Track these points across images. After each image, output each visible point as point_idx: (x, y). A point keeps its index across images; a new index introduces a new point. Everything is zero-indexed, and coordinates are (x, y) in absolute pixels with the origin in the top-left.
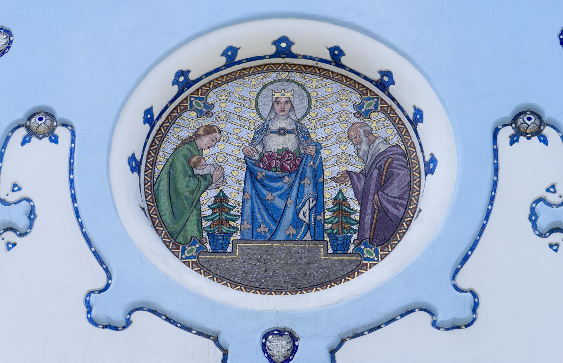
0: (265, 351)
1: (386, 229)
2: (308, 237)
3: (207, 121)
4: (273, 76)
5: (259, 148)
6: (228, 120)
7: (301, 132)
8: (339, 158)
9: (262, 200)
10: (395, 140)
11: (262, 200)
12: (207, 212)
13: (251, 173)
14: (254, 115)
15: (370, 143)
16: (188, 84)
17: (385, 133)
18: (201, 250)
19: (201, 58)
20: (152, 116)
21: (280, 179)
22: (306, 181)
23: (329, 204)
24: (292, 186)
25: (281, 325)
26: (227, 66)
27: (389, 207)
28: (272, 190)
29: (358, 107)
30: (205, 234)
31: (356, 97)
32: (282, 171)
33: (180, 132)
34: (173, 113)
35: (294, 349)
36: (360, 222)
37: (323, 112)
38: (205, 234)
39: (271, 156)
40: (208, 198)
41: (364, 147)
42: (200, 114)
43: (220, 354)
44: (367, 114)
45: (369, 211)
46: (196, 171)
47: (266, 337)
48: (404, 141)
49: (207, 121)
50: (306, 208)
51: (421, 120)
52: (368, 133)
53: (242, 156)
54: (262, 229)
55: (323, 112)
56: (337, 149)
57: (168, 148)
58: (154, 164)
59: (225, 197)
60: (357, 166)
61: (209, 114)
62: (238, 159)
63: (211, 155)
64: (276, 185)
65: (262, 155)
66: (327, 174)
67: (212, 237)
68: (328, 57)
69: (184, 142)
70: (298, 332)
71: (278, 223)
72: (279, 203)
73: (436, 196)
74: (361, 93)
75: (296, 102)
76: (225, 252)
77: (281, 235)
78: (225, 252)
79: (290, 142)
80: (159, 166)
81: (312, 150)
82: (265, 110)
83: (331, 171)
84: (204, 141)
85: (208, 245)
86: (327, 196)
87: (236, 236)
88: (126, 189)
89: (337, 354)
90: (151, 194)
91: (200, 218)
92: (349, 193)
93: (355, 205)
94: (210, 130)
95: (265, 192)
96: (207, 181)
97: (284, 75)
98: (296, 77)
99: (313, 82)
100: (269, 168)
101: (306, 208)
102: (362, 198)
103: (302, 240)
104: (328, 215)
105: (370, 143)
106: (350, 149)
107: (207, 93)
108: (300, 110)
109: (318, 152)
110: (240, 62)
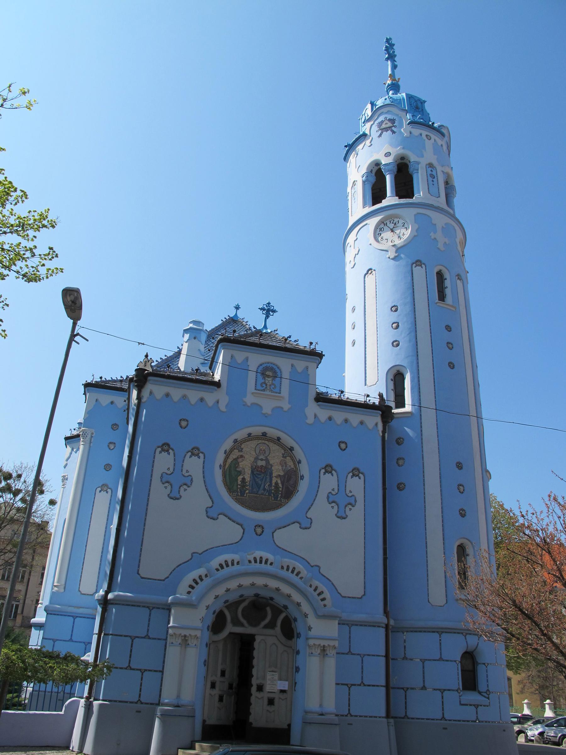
1: (289, 494)
2: (267, 494)
3: (241, 454)
4: (260, 441)
7: (267, 460)
8: (277, 470)
13: (252, 472)
14: (254, 453)
15: (286, 466)
16: (237, 442)
17: (290, 464)
18: (237, 495)
19: (241, 435)
21: (260, 475)
22: (268, 476)
23: (273, 485)
25: (260, 524)
28: (258, 478)
29: (283, 454)
31: (283, 451)
32: (261, 472)
33: (233, 456)
34: (232, 450)
35: (263, 532)
36: (281, 491)
39: (258, 467)
42: (239, 451)
44: (285, 457)
45: (284, 488)
46: (237, 469)
47: (255, 527)
49: (241, 454)
52: (285, 463)
56: (277, 467)
57: (229, 461)
58: (225, 465)
60: (282, 473)
61: (241, 451)
64: (259, 476)
66: (274, 475)
67: (241, 491)
69: (234, 459)
71: (259, 488)
72: (260, 482)
73: (303, 486)
74: (285, 450)
76: (244, 496)
78: (244, 496)
79: (263, 463)
80: (227, 467)
81: (270, 467)
82: (258, 452)
83: (274, 474)
84: (240, 460)
87: (247, 491)
88: (218, 475)
90: (224, 475)
92: (279, 482)
93: (280, 485)
94: (242, 456)
96: (240, 473)
97: (263, 441)
98: (266, 442)
99: (271, 444)
103: (265, 495)
104: (273, 488)
105: (286, 466)
106: (280, 468)
107: (241, 444)
109: (271, 467)
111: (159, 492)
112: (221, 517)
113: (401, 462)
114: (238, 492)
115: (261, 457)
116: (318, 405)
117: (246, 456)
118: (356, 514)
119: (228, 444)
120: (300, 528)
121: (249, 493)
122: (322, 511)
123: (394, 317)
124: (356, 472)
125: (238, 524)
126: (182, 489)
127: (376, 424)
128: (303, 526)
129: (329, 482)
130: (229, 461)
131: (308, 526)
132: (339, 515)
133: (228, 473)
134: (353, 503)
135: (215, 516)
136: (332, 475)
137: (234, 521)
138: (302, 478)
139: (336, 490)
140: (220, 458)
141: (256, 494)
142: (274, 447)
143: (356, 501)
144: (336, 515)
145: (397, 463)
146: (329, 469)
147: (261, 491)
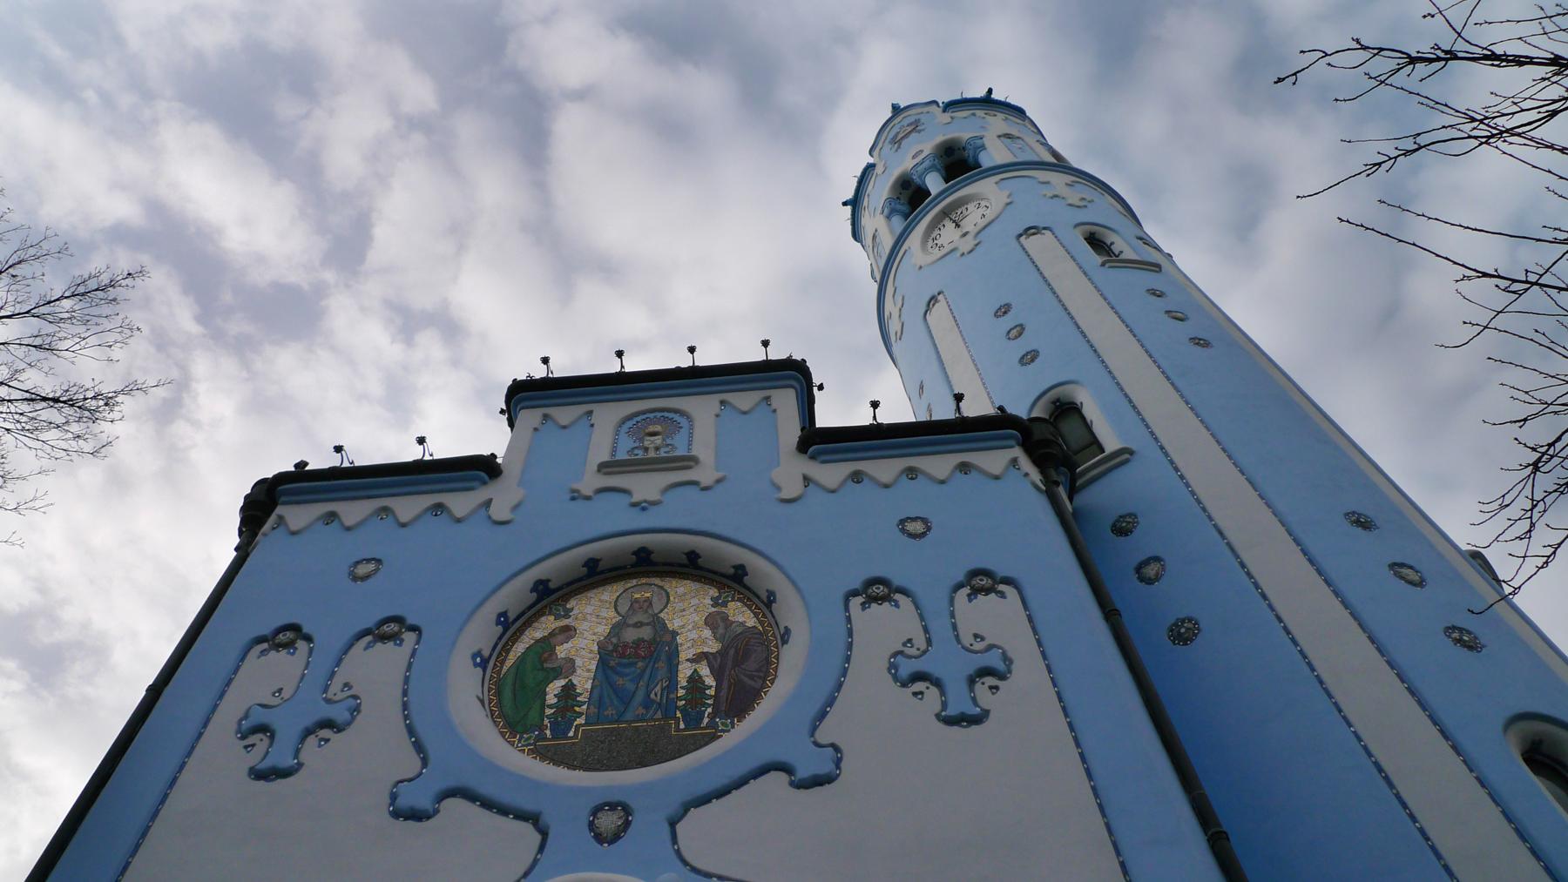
0: (591, 830)
2: (659, 715)
5: (614, 640)
6: (585, 619)
7: (658, 624)
9: (611, 685)
10: (751, 622)
11: (611, 685)
12: (551, 699)
13: (603, 663)
14: (612, 613)
20: (506, 618)
22: (660, 664)
24: (644, 671)
25: (616, 798)
26: (589, 576)
27: (746, 679)
28: (622, 675)
30: (546, 721)
32: (637, 656)
35: (627, 824)
37: (680, 606)
38: (546, 721)
39: (626, 646)
40: (555, 687)
41: (721, 631)
43: (538, 838)
44: (725, 604)
48: (762, 623)
50: (658, 688)
51: (774, 601)
53: (595, 648)
54: (609, 712)
55: (680, 606)
56: (693, 635)
57: (520, 648)
58: (503, 663)
59: (573, 686)
60: (713, 647)
61: (567, 616)
62: (591, 652)
63: (562, 651)
65: (616, 646)
66: (683, 656)
67: (555, 726)
68: (686, 561)
69: (537, 641)
70: (633, 804)
72: (631, 686)
73: (792, 663)
75: (655, 600)
77: (629, 716)
79: (646, 633)
83: (685, 653)
84: (560, 638)
85: (548, 732)
86: (681, 675)
87: (578, 721)
89: (679, 827)
91: (543, 706)
92: (704, 671)
93: (710, 681)
95: (616, 678)
96: (557, 673)
98: (657, 581)
100: (623, 656)
101: (658, 688)
102: (717, 673)
106: (707, 633)
108: (657, 607)
110: (602, 572)
111: (221, 759)
112: (454, 805)
113: (1151, 571)
114: (541, 728)
115: (640, 617)
116: (812, 458)
117: (582, 626)
118: (1024, 700)
119: (515, 595)
120: (793, 784)
121: (586, 724)
122: (879, 721)
123: (1008, 322)
124: (981, 582)
125: (521, 816)
126: (312, 740)
127: (1014, 462)
128: (803, 772)
129: (884, 628)
130: (520, 648)
131: (826, 768)
132: (952, 711)
133: (509, 681)
134: (1001, 666)
135: (425, 803)
136: (897, 606)
137: (504, 811)
138: (785, 636)
139: (920, 642)
140: (481, 633)
141: (617, 721)
142: (680, 589)
143: (1007, 660)
144: (938, 716)
145: (1142, 579)
146: (877, 591)
147: (636, 709)
